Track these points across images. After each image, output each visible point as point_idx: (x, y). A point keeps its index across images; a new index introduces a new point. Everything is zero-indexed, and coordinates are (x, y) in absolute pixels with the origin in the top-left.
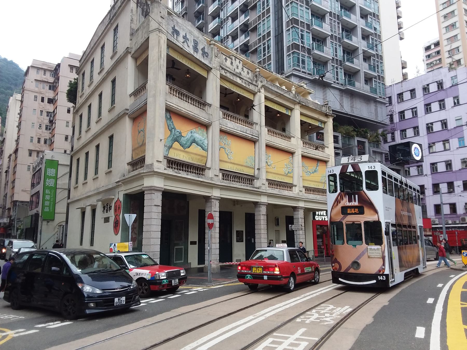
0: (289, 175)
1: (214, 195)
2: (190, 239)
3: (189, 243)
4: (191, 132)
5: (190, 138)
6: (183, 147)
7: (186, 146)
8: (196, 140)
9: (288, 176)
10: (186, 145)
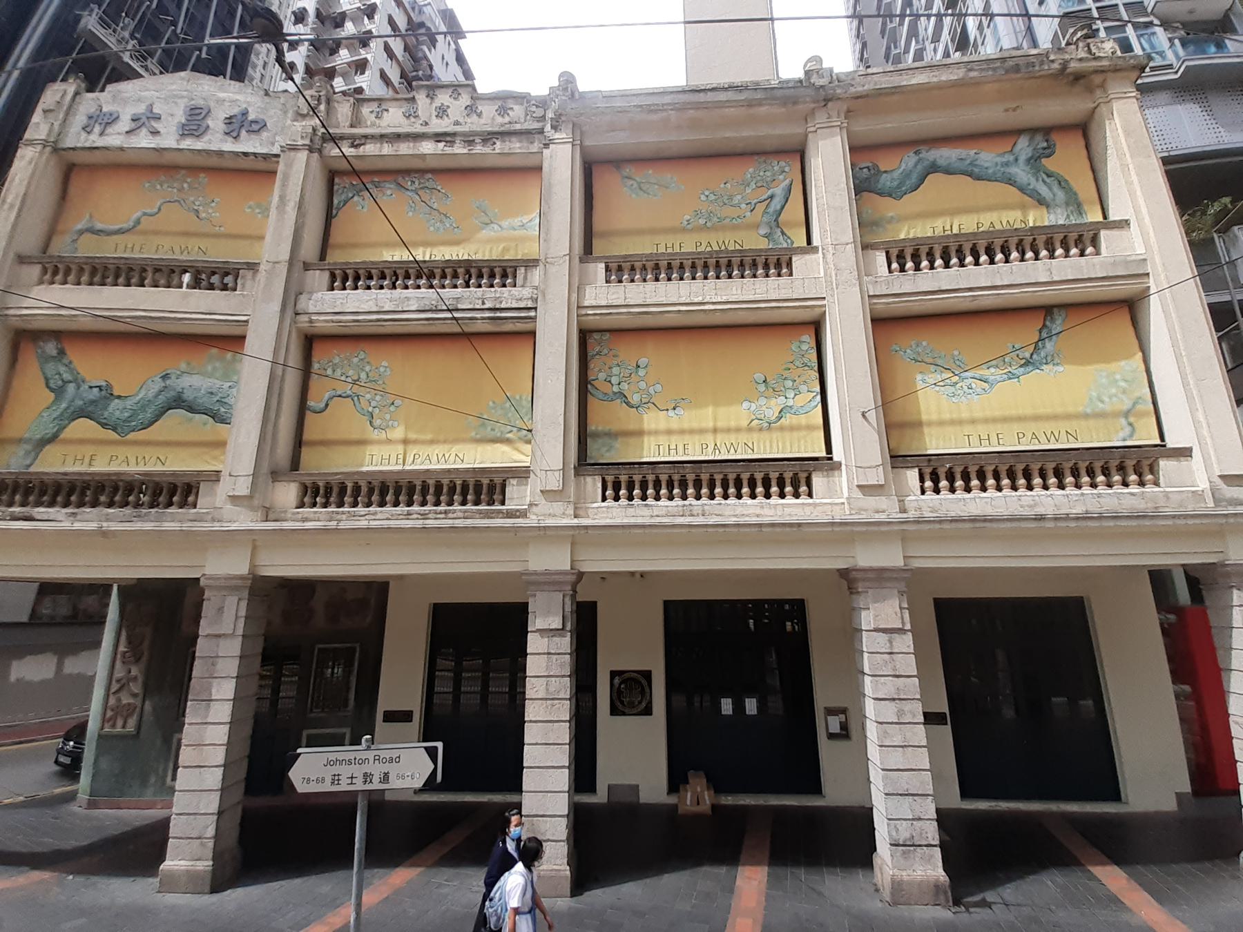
0: (787, 420)
1: (209, 571)
2: (385, 702)
3: (379, 716)
4: (165, 377)
5: (156, 396)
6: (114, 429)
7: (134, 423)
8: (188, 395)
9: (782, 429)
10: (129, 422)
